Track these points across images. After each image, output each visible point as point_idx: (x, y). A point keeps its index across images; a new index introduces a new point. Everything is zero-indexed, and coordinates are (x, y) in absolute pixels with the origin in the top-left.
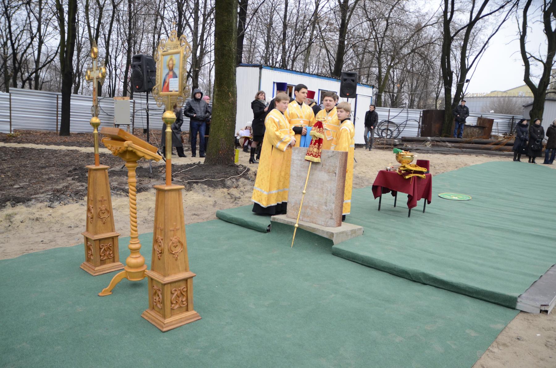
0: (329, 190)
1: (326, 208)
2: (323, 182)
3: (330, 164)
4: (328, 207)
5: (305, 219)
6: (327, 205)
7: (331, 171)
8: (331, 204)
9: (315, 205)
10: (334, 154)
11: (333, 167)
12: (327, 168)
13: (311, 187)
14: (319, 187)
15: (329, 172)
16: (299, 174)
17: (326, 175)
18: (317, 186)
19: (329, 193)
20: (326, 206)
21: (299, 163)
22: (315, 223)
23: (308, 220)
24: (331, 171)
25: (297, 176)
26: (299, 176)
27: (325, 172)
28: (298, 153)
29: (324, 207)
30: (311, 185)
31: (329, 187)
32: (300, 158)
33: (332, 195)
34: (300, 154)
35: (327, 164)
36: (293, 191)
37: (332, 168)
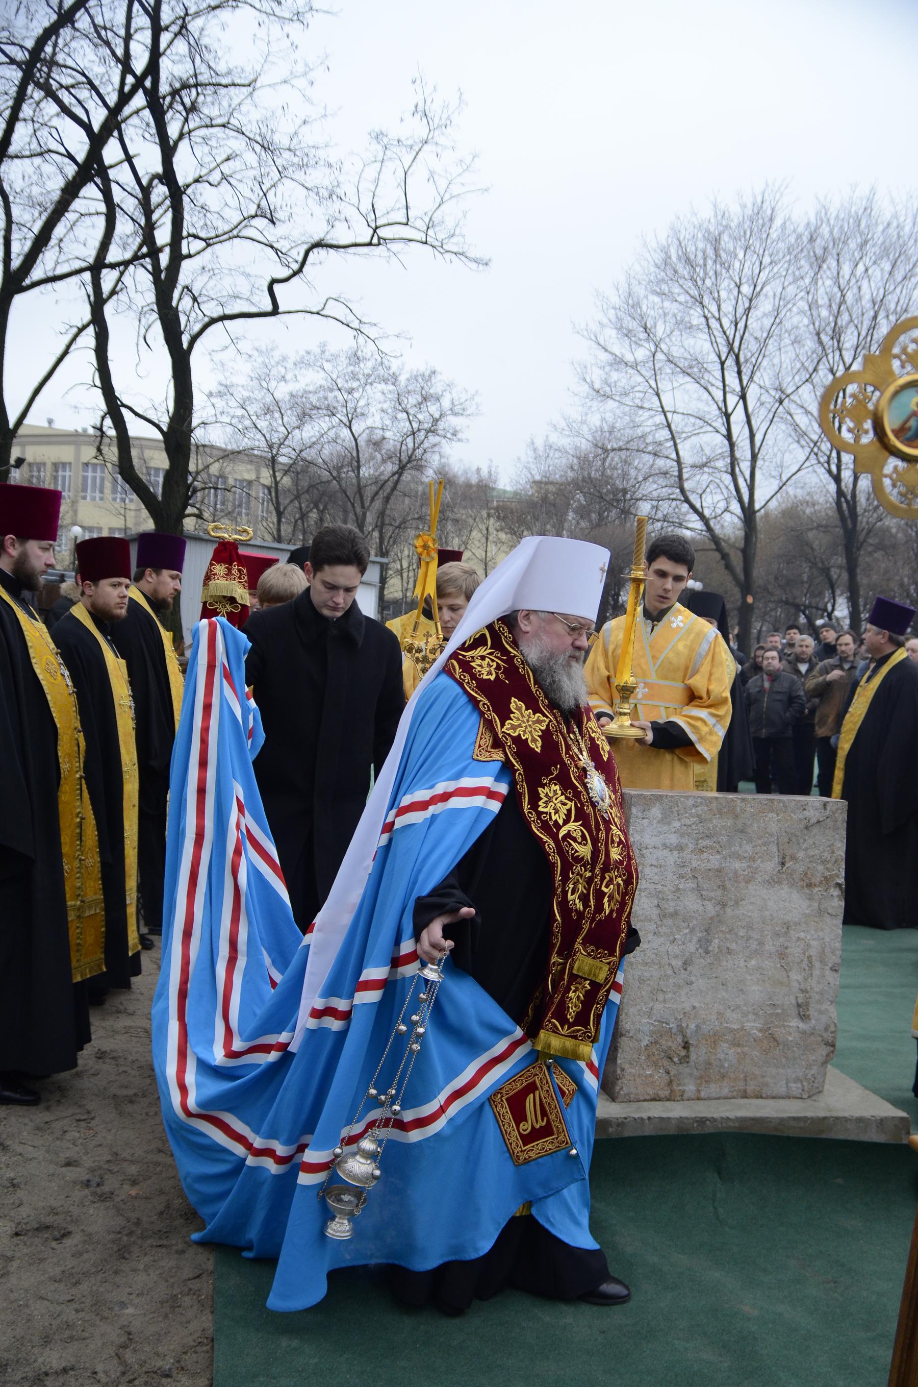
0: (813, 952)
1: (802, 1026)
2: (788, 926)
3: (811, 853)
4: (813, 1022)
5: (713, 1089)
6: (812, 1012)
7: (816, 880)
8: (823, 1007)
9: (748, 1025)
10: (828, 813)
11: (824, 862)
12: (800, 868)
13: (729, 951)
14: (769, 947)
15: (809, 885)
16: (670, 907)
17: (795, 896)
18: (761, 944)
19: (817, 965)
20: (804, 1017)
21: (672, 858)
22: (759, 1097)
23: (725, 1091)
24: (816, 880)
25: (663, 916)
26: (675, 914)
27: (792, 885)
28: (665, 819)
29: (795, 1023)
30: (733, 946)
31: (814, 943)
32: (673, 839)
33: (828, 972)
34: (677, 824)
35: (801, 855)
36: (642, 981)
37: (820, 868)
